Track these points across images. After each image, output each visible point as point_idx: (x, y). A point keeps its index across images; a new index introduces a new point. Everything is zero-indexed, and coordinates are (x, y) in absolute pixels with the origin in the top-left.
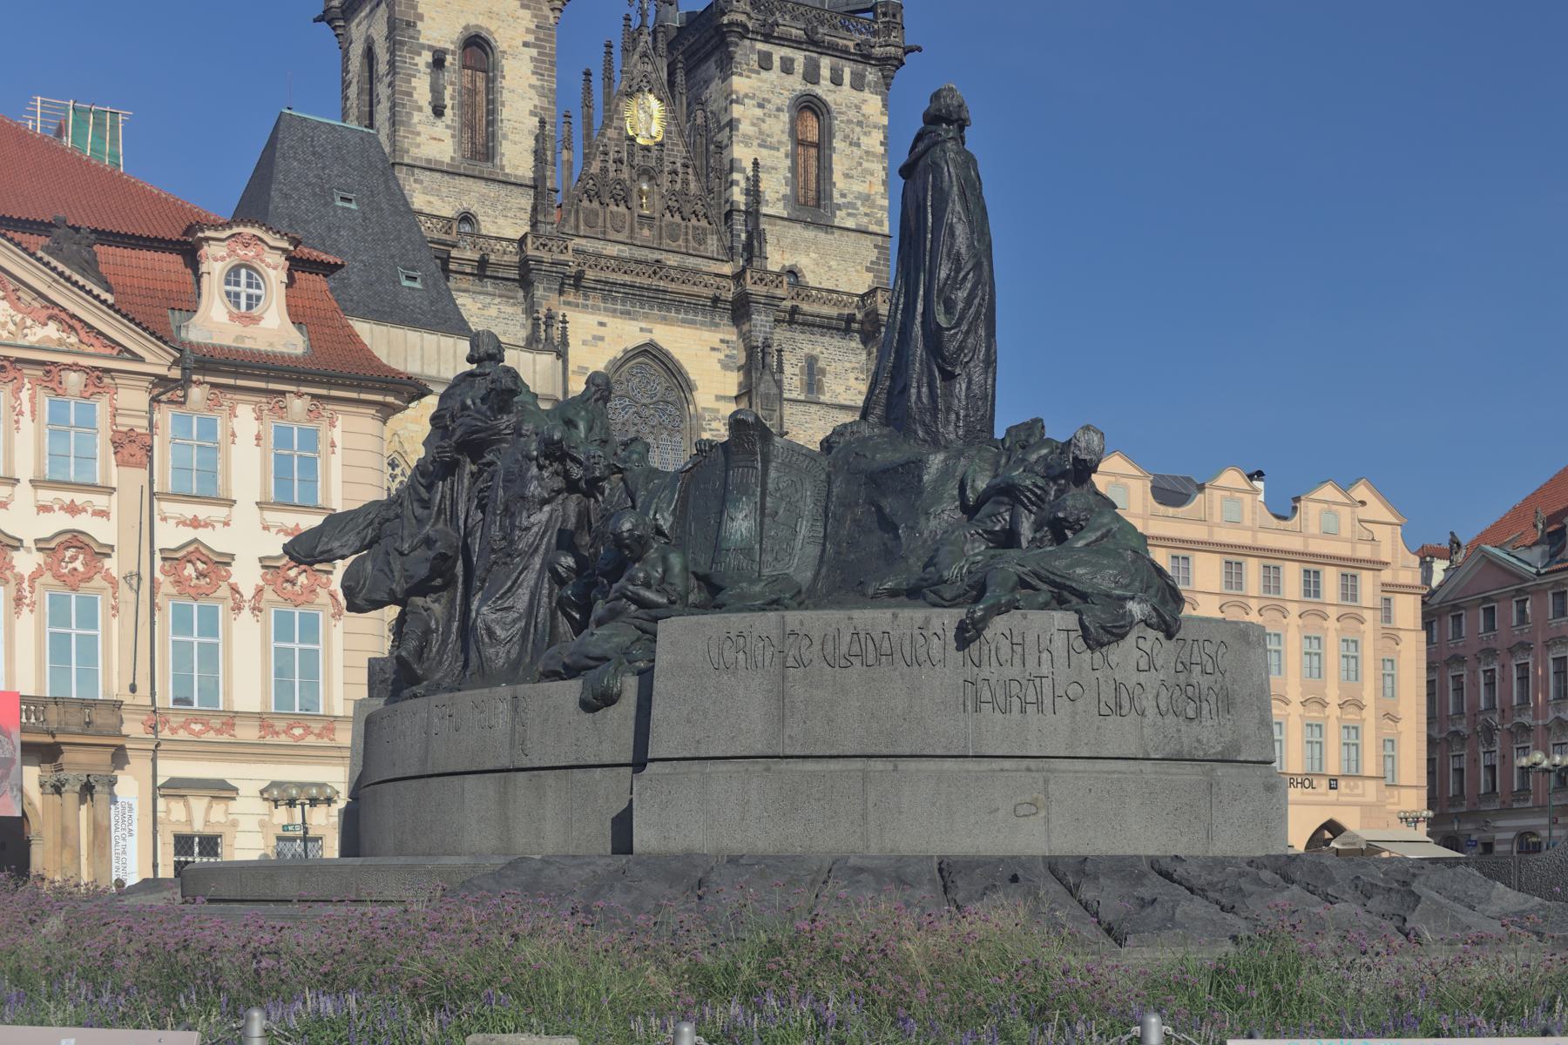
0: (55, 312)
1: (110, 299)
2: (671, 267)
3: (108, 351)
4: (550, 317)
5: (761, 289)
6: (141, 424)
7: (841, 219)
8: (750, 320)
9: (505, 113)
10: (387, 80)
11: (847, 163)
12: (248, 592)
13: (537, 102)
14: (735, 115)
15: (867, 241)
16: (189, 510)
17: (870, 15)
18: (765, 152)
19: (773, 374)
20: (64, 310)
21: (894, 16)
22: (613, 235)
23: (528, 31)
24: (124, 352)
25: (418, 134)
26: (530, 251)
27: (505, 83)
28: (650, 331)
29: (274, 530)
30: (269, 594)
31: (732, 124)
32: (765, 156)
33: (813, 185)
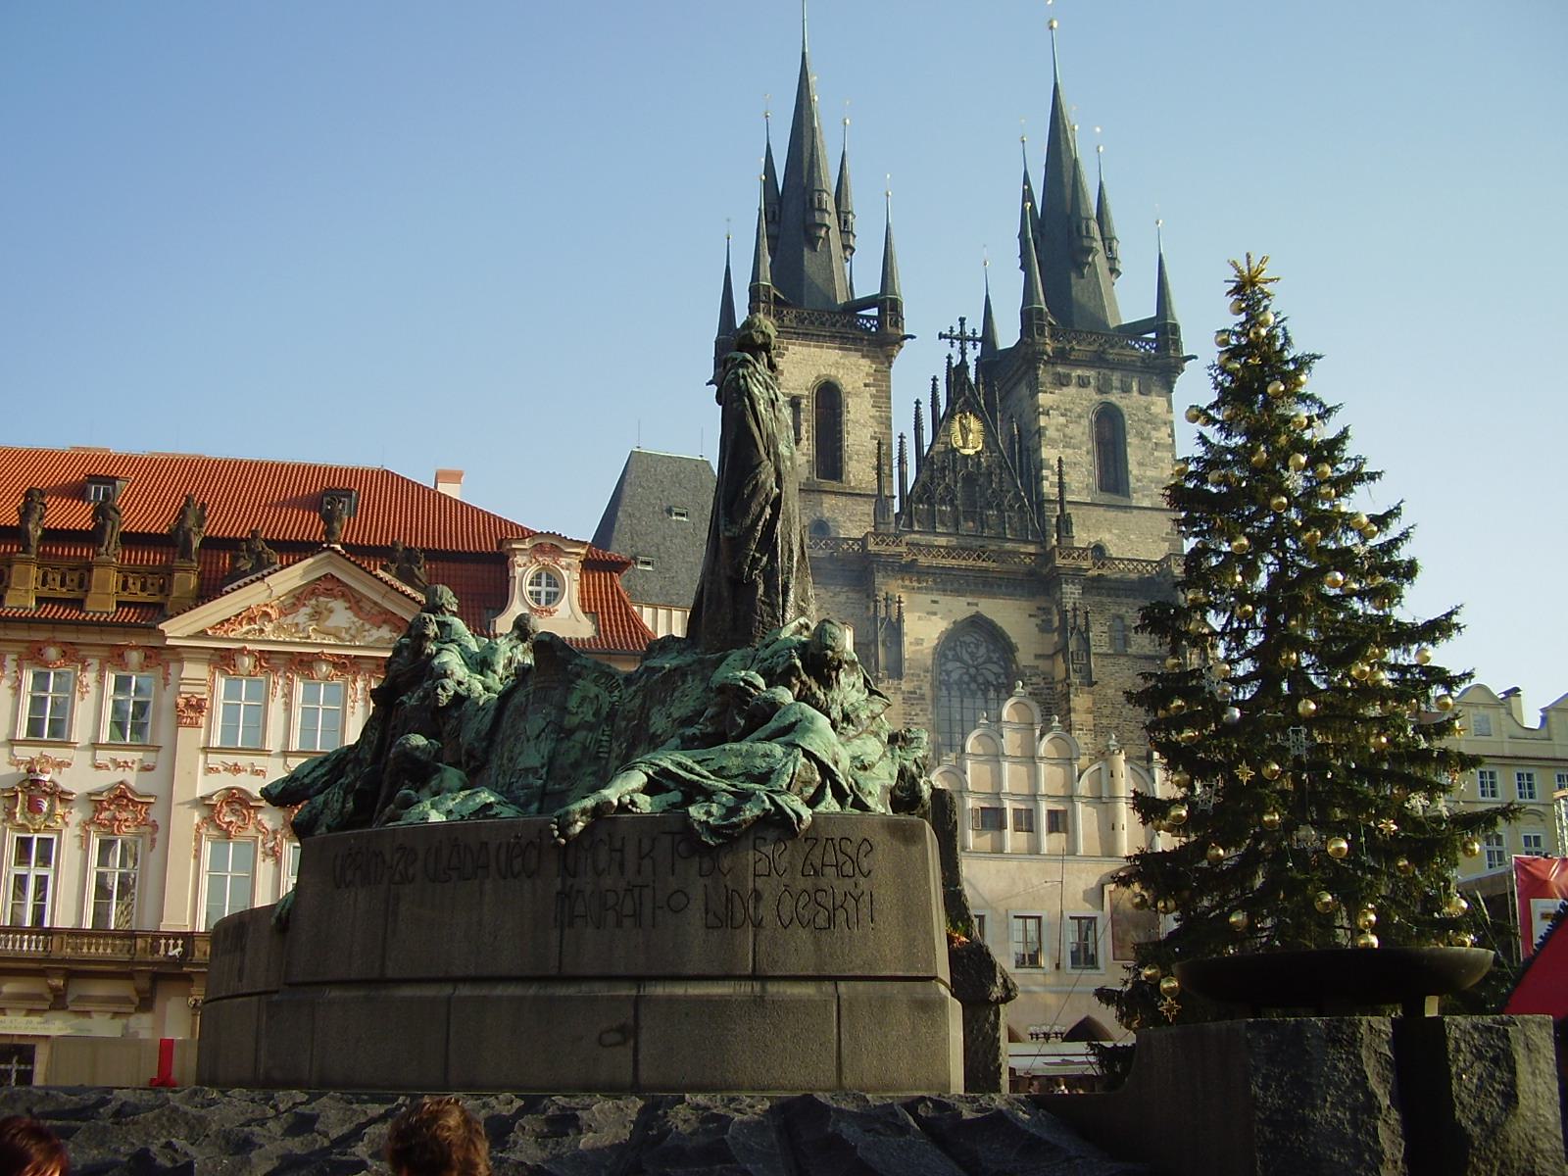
5: (1069, 561)
7: (1137, 500)
14: (1042, 424)
17: (1153, 335)
18: (1069, 451)
26: (872, 547)
27: (851, 416)
28: (977, 605)
31: (1040, 432)
32: (1068, 454)
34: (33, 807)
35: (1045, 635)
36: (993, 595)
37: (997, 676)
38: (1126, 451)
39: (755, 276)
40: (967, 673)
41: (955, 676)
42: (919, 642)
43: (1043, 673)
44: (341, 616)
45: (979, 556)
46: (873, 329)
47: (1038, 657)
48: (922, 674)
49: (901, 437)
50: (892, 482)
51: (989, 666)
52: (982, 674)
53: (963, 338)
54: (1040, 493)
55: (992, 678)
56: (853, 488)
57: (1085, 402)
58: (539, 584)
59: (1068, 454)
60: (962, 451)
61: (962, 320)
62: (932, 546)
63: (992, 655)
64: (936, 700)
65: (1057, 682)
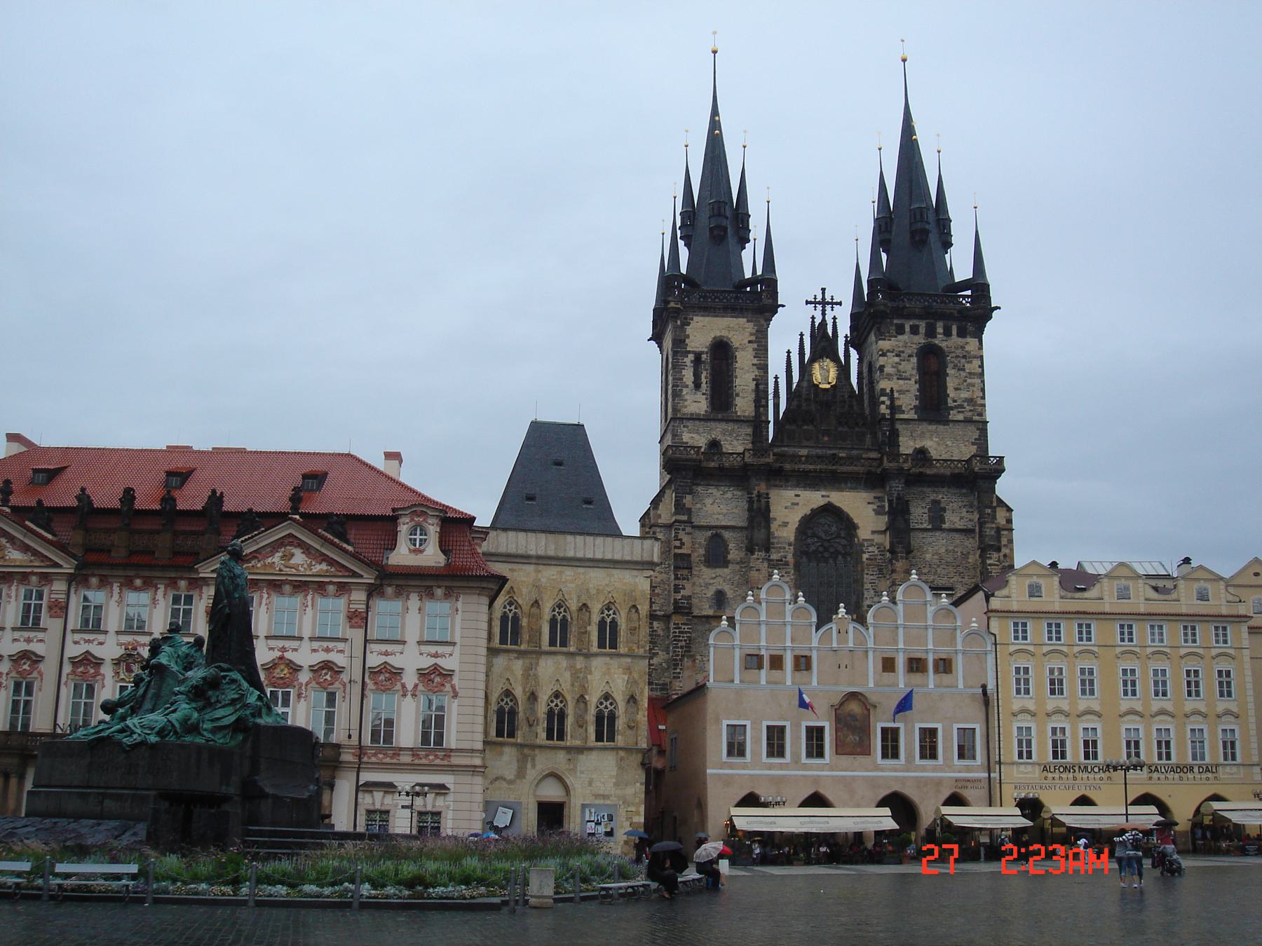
0: (325, 558)
1: (350, 548)
6: (362, 607)
7: (955, 415)
9: (738, 382)
11: (957, 381)
12: (410, 687)
15: (972, 428)
16: (383, 648)
17: (969, 293)
22: (805, 443)
24: (355, 575)
26: (746, 459)
30: (420, 687)
31: (882, 368)
34: (129, 670)
41: (813, 548)
42: (785, 524)
44: (299, 558)
47: (873, 532)
49: (776, 378)
53: (824, 303)
55: (840, 548)
61: (823, 290)
64: (797, 566)
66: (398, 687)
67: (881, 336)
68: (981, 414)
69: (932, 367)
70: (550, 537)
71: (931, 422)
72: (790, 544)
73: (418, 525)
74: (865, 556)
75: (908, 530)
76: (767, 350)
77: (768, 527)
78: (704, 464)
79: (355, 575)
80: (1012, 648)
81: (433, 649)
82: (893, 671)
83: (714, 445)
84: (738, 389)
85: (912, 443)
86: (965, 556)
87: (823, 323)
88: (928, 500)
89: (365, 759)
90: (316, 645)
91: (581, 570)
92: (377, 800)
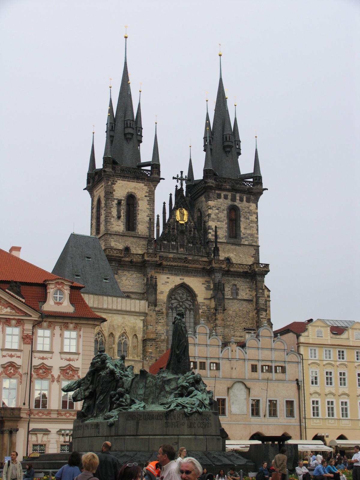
1: (24, 301)
2: (189, 260)
3: (22, 314)
4: (152, 277)
8: (214, 275)
10: (104, 209)
12: (56, 376)
13: (149, 213)
14: (210, 212)
15: (252, 249)
16: (42, 355)
17: (251, 180)
18: (219, 223)
19: (221, 292)
20: (12, 304)
21: (259, 180)
23: (146, 192)
24: (26, 315)
25: (113, 224)
26: (146, 258)
27: (140, 208)
28: (183, 279)
29: (64, 360)
30: (62, 377)
31: (209, 215)
32: (219, 224)
33: (234, 232)
35: (208, 291)
36: (189, 276)
37: (190, 305)
38: (240, 223)
39: (105, 154)
40: (179, 304)
41: (175, 305)
42: (162, 293)
43: (206, 305)
45: (185, 262)
46: (149, 175)
47: (205, 299)
48: (163, 304)
49: (158, 216)
50: (154, 233)
51: (187, 302)
52: (184, 305)
53: (182, 179)
54: (208, 238)
55: (188, 306)
56: (140, 235)
57: (225, 205)
58: (57, 294)
59: (219, 224)
60: (180, 222)
61: (182, 172)
62: (168, 258)
63: (188, 298)
64: (167, 314)
65: (212, 308)
66: (50, 376)
67: (208, 199)
68: (256, 242)
69: (234, 216)
70: (96, 297)
71: (233, 244)
72: (164, 303)
73: (59, 289)
74: (201, 311)
75: (224, 298)
76: (154, 201)
77: (156, 294)
78: (123, 259)
79: (26, 315)
80: (310, 362)
81: (68, 356)
82: (256, 372)
83: (127, 249)
84: (139, 220)
85: (223, 254)
86: (248, 313)
87: (182, 189)
88: (231, 284)
89: (32, 416)
90: (5, 353)
91: (110, 315)
92: (40, 438)
